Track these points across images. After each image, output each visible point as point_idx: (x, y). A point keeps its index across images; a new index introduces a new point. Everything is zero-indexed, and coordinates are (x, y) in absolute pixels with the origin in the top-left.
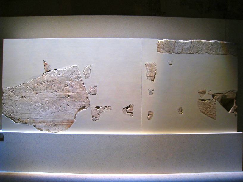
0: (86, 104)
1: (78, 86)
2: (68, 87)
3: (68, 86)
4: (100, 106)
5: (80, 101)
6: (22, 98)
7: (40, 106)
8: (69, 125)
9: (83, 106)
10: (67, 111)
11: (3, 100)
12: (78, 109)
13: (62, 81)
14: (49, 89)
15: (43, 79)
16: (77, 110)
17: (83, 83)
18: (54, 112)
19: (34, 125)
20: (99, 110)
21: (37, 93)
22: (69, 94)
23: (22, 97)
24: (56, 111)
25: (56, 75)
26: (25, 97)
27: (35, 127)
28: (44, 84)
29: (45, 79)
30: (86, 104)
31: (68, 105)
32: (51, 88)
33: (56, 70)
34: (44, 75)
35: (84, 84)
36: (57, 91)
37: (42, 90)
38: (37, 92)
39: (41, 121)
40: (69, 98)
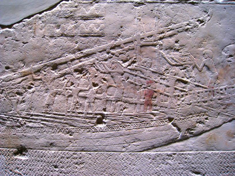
14: (131, 110)
15: (70, 26)
21: (22, 150)
28: (80, 71)
29: (91, 26)
32: (149, 104)
36: (200, 127)
38: (23, 142)
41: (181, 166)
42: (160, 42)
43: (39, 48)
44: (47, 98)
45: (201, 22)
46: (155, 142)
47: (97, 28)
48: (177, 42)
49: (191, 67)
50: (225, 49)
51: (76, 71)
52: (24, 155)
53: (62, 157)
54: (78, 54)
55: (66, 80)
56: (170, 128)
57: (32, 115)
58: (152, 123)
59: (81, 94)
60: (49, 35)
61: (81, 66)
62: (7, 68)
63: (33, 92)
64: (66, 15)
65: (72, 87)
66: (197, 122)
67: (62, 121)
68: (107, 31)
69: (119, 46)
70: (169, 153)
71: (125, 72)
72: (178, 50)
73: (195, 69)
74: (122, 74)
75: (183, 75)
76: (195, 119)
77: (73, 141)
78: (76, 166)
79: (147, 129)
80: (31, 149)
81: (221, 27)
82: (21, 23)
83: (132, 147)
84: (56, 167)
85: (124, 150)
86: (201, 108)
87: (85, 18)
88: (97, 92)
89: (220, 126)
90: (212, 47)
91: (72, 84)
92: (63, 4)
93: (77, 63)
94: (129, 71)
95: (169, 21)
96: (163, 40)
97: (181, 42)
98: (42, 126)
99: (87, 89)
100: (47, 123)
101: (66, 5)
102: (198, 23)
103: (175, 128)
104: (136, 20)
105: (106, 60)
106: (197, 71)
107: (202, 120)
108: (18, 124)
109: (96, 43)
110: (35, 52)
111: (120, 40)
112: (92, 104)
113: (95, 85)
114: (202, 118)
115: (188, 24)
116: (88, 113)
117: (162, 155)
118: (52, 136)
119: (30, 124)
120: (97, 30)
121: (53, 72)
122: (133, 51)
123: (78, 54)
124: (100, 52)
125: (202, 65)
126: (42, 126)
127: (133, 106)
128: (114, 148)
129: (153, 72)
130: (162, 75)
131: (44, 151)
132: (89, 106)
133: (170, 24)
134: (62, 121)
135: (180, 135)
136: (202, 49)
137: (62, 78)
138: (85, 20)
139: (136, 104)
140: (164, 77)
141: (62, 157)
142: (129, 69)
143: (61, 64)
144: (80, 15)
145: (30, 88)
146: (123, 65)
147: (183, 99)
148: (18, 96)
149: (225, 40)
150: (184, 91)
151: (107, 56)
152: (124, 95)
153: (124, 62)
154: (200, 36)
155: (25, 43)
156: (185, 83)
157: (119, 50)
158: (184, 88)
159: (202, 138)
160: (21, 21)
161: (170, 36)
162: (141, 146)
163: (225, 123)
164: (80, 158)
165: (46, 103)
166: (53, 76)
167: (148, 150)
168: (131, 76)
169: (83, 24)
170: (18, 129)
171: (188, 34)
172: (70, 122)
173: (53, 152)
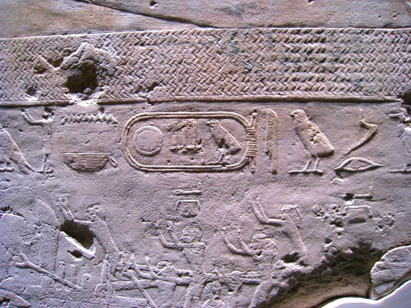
0: (386, 211)
9: (344, 242)
30: (386, 211)
31: (84, 235)
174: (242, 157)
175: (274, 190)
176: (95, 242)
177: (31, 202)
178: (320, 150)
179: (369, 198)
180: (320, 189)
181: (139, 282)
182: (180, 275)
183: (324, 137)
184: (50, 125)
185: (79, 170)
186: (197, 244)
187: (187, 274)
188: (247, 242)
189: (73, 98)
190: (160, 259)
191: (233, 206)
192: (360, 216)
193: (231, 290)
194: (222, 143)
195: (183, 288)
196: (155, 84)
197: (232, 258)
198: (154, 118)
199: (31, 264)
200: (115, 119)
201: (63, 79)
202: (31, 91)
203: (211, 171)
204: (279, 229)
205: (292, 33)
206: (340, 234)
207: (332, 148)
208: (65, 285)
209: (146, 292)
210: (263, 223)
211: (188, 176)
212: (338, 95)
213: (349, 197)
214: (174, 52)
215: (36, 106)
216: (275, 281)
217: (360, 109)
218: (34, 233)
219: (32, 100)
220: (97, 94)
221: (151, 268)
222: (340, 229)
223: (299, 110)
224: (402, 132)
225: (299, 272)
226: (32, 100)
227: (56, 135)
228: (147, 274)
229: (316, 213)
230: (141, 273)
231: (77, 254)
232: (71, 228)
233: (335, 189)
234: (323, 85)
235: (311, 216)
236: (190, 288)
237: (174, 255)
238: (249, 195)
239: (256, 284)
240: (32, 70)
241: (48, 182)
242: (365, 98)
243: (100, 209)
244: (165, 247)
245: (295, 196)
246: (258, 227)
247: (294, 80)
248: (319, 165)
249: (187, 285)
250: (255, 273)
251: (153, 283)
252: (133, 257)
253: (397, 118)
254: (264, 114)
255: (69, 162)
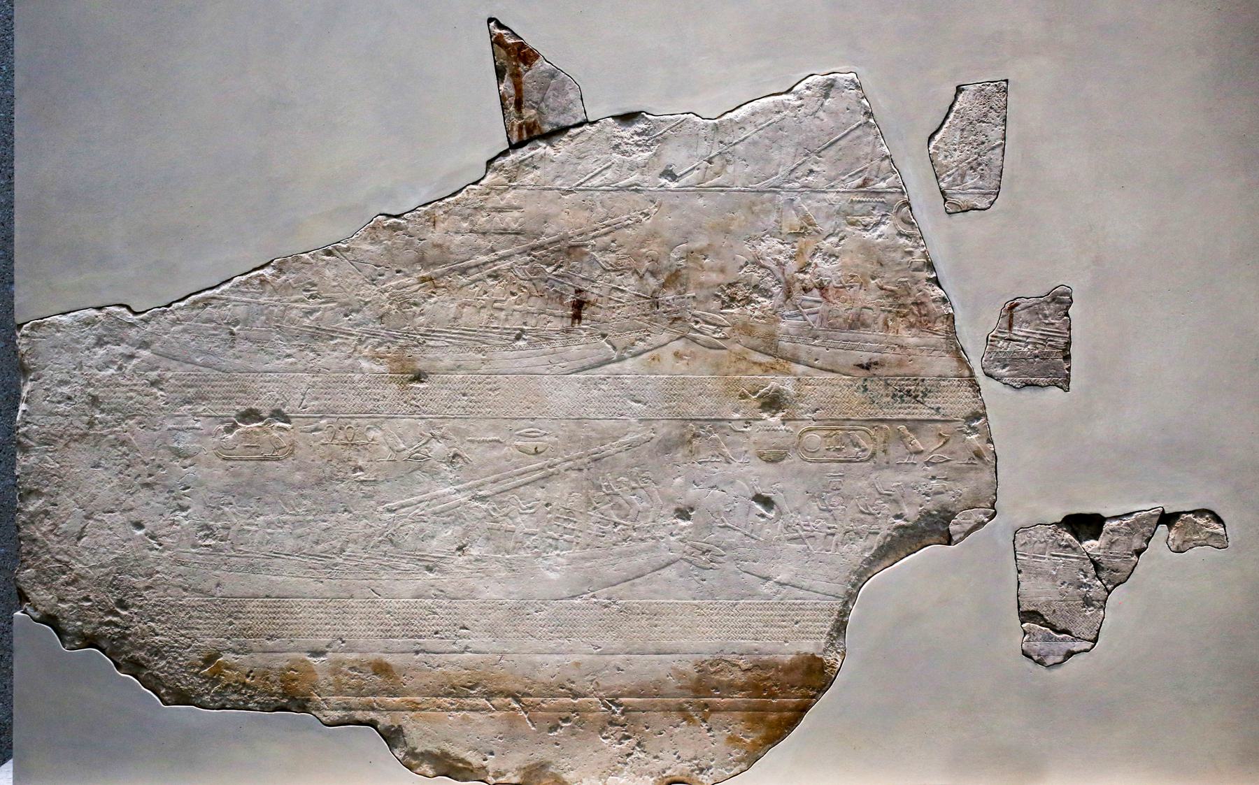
1: (869, 298)
2: (767, 303)
3: (766, 293)
4: (1106, 513)
5: (896, 451)
6: (243, 427)
7: (451, 515)
8: (773, 716)
10: (757, 567)
11: (26, 450)
12: (876, 542)
13: (700, 242)
16: (860, 550)
17: (930, 266)
18: (611, 572)
19: (384, 720)
20: (1091, 545)
21: (418, 377)
22: (774, 382)
23: (250, 415)
24: (640, 560)
25: (634, 177)
26: (278, 414)
27: (392, 737)
28: (495, 276)
31: (767, 502)
33: (627, 118)
34: (490, 178)
35: (942, 271)
37: (476, 339)
38: (420, 365)
39: (465, 675)
40: (771, 430)
41: (617, 393)
42: (593, 242)
43: (439, 246)
44: (453, 310)
45: (647, 215)
46: (585, 363)
47: (515, 223)
48: (613, 241)
49: (630, 273)
50: (675, 250)
51: (489, 276)
52: (422, 382)
53: (472, 383)
54: (492, 256)
55: (477, 288)
56: (603, 346)
57: (434, 331)
58: (582, 340)
59: (496, 305)
60: (454, 230)
61: (495, 271)
62: (398, 272)
63: (435, 303)
64: (475, 205)
65: (484, 297)
66: (636, 340)
67: (473, 338)
68: (528, 227)
69: (541, 247)
70: (603, 376)
71: (549, 279)
72: (614, 252)
73: (636, 275)
74: (546, 281)
75: (619, 283)
76: (635, 335)
77: (486, 362)
78: (490, 392)
79: (576, 347)
80: (433, 374)
81: (672, 222)
82: (414, 213)
83: (557, 369)
84: (464, 395)
85: (548, 372)
86: (641, 323)
87: (500, 210)
88: (516, 303)
89: (666, 344)
90: (658, 247)
91: (485, 293)
92: (472, 189)
93: (490, 268)
94: (554, 278)
95: (605, 215)
96: (597, 239)
97: (620, 240)
98: (447, 344)
99: (504, 299)
100: (453, 341)
101: (475, 191)
102: (641, 217)
103: (608, 345)
104: (563, 213)
105: (526, 264)
106: (637, 277)
107: (643, 337)
108: (416, 343)
109: (514, 242)
110: (436, 252)
111: (544, 239)
112: (509, 317)
113: (513, 294)
114: (642, 335)
115: (629, 219)
116: (505, 329)
117: (594, 379)
118: (460, 357)
119: (431, 343)
120: (515, 226)
121: (461, 277)
122: (559, 254)
123: (492, 256)
124: (519, 254)
125: (644, 270)
126: (447, 344)
127: (559, 319)
128: (537, 370)
129: (583, 279)
130: (593, 282)
131: (449, 376)
132: (507, 320)
133: (604, 220)
134: (473, 338)
135: (615, 355)
136: (644, 250)
137: (473, 285)
138: (499, 212)
139: (562, 317)
140: (596, 285)
141: (472, 383)
142: (555, 275)
143: (471, 268)
144: (493, 205)
145: (430, 297)
146: (547, 270)
147: (619, 311)
148: (415, 308)
149: (676, 239)
150: (621, 302)
151: (528, 258)
152: (548, 306)
153: (549, 265)
154: (643, 233)
155: (422, 240)
156: (622, 291)
157: (543, 252)
158: (620, 298)
159: (643, 359)
160: (414, 210)
161: (606, 234)
162: (568, 368)
163: (671, 341)
164: (495, 383)
165: (452, 316)
166: (460, 284)
167: (577, 372)
168: (556, 284)
169: (497, 217)
170: (416, 349)
171: (628, 231)
172: (481, 338)
173: (461, 376)
174: (869, 453)
175: (888, 473)
176: (775, 507)
177: (732, 482)
178: (915, 450)
179: (946, 479)
180: (916, 473)
181: (803, 533)
182: (829, 528)
183: (918, 442)
184: (749, 432)
185: (766, 461)
186: (840, 507)
187: (834, 527)
188: (872, 506)
189: (765, 415)
190: (817, 518)
191: (863, 484)
192: (940, 490)
193: (861, 538)
194: (857, 445)
195: (830, 537)
196: (818, 409)
197: (862, 516)
198: (816, 429)
199: (729, 525)
200: (792, 430)
201: (759, 404)
202: (736, 411)
203: (850, 461)
204: (891, 498)
205: (899, 380)
206: (928, 501)
207: (922, 448)
208: (752, 538)
209: (807, 541)
210: (880, 494)
211: (835, 465)
212: (925, 417)
213: (934, 478)
214: (828, 390)
215: (739, 420)
216: (889, 532)
217: (939, 425)
218: (733, 503)
219: (737, 416)
220: (780, 414)
221: (811, 523)
222: (929, 498)
223: (902, 427)
224: (965, 439)
225: (903, 525)
226: (737, 416)
227: (753, 439)
228: (808, 528)
229: (913, 488)
230: (805, 528)
231: (763, 516)
232: (759, 498)
233: (924, 473)
234: (917, 411)
235: (910, 490)
236: (836, 537)
237: (827, 514)
238: (873, 476)
239: (878, 533)
240: (737, 397)
241: (746, 469)
242: (942, 419)
243: (780, 486)
244: (820, 509)
245: (901, 477)
246: (877, 496)
247: (900, 408)
248: (915, 459)
249: (833, 535)
250: (876, 527)
251: (812, 534)
252: (799, 517)
253: (962, 431)
254: (882, 428)
255: (760, 456)
